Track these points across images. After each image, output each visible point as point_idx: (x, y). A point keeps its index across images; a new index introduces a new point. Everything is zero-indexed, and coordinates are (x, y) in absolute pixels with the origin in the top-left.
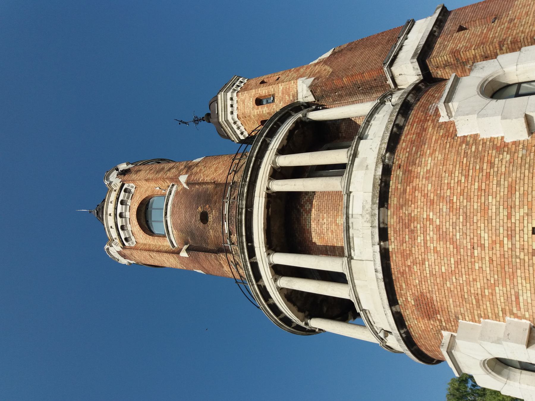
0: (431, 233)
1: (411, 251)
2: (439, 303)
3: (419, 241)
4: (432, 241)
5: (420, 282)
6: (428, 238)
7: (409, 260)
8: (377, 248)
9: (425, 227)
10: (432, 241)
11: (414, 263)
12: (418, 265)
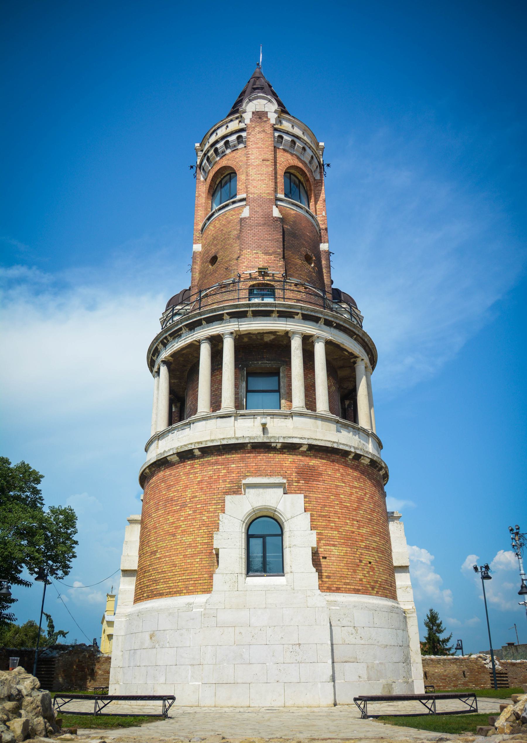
0: (360, 493)
1: (349, 475)
2: (316, 485)
3: (355, 483)
4: (356, 492)
5: (329, 475)
6: (358, 490)
7: (343, 471)
8: (353, 450)
9: (362, 490)
10: (356, 492)
11: (342, 475)
12: (341, 477)
